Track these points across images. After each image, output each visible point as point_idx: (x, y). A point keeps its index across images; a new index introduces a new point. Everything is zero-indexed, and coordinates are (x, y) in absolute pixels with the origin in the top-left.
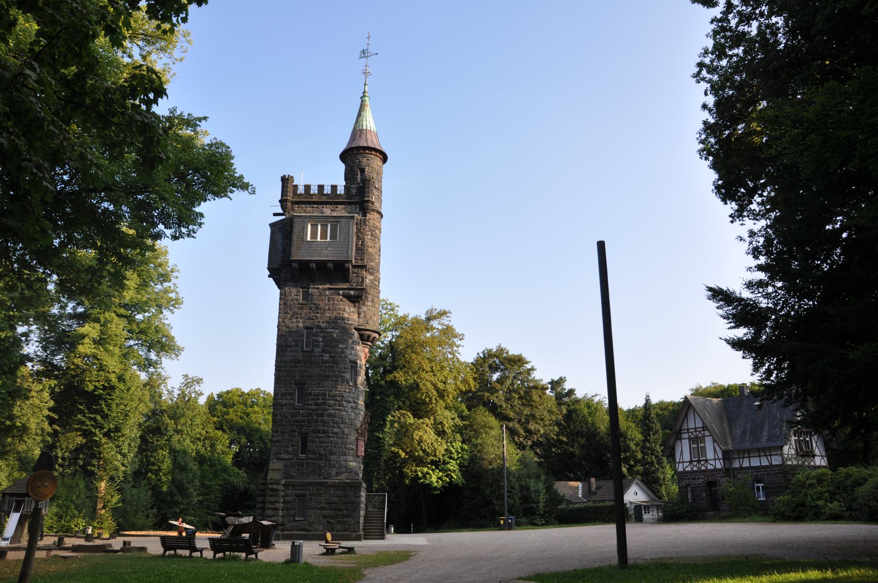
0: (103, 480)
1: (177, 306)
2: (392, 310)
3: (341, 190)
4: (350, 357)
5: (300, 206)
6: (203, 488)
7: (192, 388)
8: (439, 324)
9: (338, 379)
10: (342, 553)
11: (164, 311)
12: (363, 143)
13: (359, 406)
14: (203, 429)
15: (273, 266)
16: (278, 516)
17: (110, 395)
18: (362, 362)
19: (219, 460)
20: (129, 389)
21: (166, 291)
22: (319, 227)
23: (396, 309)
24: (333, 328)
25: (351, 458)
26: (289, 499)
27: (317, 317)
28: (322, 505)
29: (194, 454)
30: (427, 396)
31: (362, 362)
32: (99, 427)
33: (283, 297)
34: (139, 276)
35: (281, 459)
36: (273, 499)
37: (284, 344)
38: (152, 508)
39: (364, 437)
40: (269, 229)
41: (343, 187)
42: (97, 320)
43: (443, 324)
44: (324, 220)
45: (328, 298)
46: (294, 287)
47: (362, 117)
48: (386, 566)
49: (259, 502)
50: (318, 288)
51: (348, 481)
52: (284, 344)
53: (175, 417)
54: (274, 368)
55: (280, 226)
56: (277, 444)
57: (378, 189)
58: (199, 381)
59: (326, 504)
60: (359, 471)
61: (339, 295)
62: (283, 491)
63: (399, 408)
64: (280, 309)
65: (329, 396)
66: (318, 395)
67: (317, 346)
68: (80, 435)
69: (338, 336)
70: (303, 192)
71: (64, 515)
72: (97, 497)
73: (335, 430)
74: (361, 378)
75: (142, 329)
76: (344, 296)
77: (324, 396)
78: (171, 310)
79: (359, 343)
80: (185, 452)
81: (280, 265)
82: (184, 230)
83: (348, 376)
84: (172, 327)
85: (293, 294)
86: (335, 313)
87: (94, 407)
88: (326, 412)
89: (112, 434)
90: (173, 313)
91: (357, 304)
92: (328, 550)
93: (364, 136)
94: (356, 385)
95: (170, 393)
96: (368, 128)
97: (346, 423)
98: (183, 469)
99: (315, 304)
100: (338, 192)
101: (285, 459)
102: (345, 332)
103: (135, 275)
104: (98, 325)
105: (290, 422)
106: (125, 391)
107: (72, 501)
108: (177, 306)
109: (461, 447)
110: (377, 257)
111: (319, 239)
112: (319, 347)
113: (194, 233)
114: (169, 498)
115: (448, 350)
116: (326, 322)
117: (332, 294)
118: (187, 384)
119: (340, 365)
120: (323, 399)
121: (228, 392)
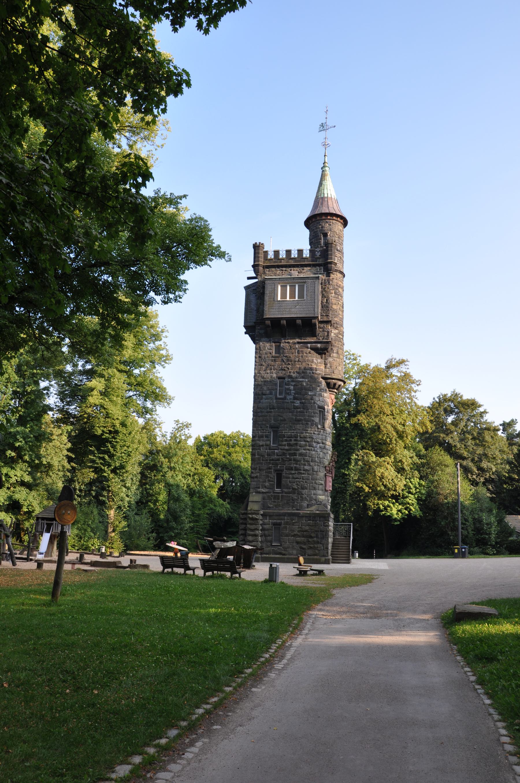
0: (112, 508)
1: (167, 362)
2: (355, 359)
3: (306, 254)
4: (318, 403)
5: (271, 269)
6: (193, 516)
7: (182, 432)
8: (398, 371)
9: (308, 422)
10: (313, 575)
11: (156, 366)
12: (325, 210)
13: (327, 447)
14: (192, 466)
15: (249, 324)
16: (257, 541)
17: (115, 439)
18: (329, 407)
19: (206, 493)
20: (130, 433)
21: (158, 349)
22: (288, 287)
23: (358, 358)
24: (303, 378)
25: (320, 492)
26: (266, 527)
27: (288, 368)
28: (296, 533)
29: (185, 488)
30: (387, 437)
31: (329, 407)
32: (107, 465)
33: (258, 351)
34: (135, 336)
35: (259, 493)
36: (253, 527)
37: (260, 392)
38: (152, 532)
39: (332, 473)
40: (243, 293)
41: (308, 251)
42: (102, 376)
43: (401, 372)
44: (292, 281)
45: (298, 351)
46: (267, 342)
47: (323, 186)
48: (352, 587)
49: (242, 529)
50: (289, 343)
51: (318, 512)
52: (260, 392)
53: (168, 456)
54: (252, 413)
55: (254, 288)
56: (255, 479)
57: (339, 251)
58: (188, 426)
59: (298, 531)
60: (327, 503)
61: (308, 348)
62: (261, 520)
63: (363, 448)
64: (255, 362)
65: (301, 438)
66: (290, 437)
67: (289, 394)
68: (92, 471)
69: (308, 385)
70: (273, 257)
71: (83, 536)
72: (108, 522)
73: (306, 467)
74: (329, 422)
75: (138, 382)
76: (311, 349)
77: (296, 437)
78: (162, 365)
79: (326, 390)
80: (178, 486)
81: (255, 323)
82: (171, 296)
83: (317, 420)
84: (164, 380)
85: (266, 348)
86: (304, 364)
87: (102, 449)
88: (298, 452)
89: (118, 471)
90: (164, 368)
91: (323, 356)
92: (300, 571)
93: (325, 203)
94: (324, 427)
95: (163, 436)
96: (329, 196)
97: (315, 461)
98: (177, 500)
99: (286, 357)
100: (304, 256)
101: (263, 493)
102: (313, 380)
103: (132, 336)
104: (103, 379)
105: (267, 460)
106: (127, 435)
107: (88, 525)
108: (167, 362)
109: (419, 483)
110: (341, 313)
111: (288, 299)
112: (291, 395)
113: (180, 298)
114: (165, 525)
115: (407, 395)
116: (296, 372)
117: (301, 347)
118: (178, 428)
119: (310, 410)
120: (295, 440)
121: (212, 435)
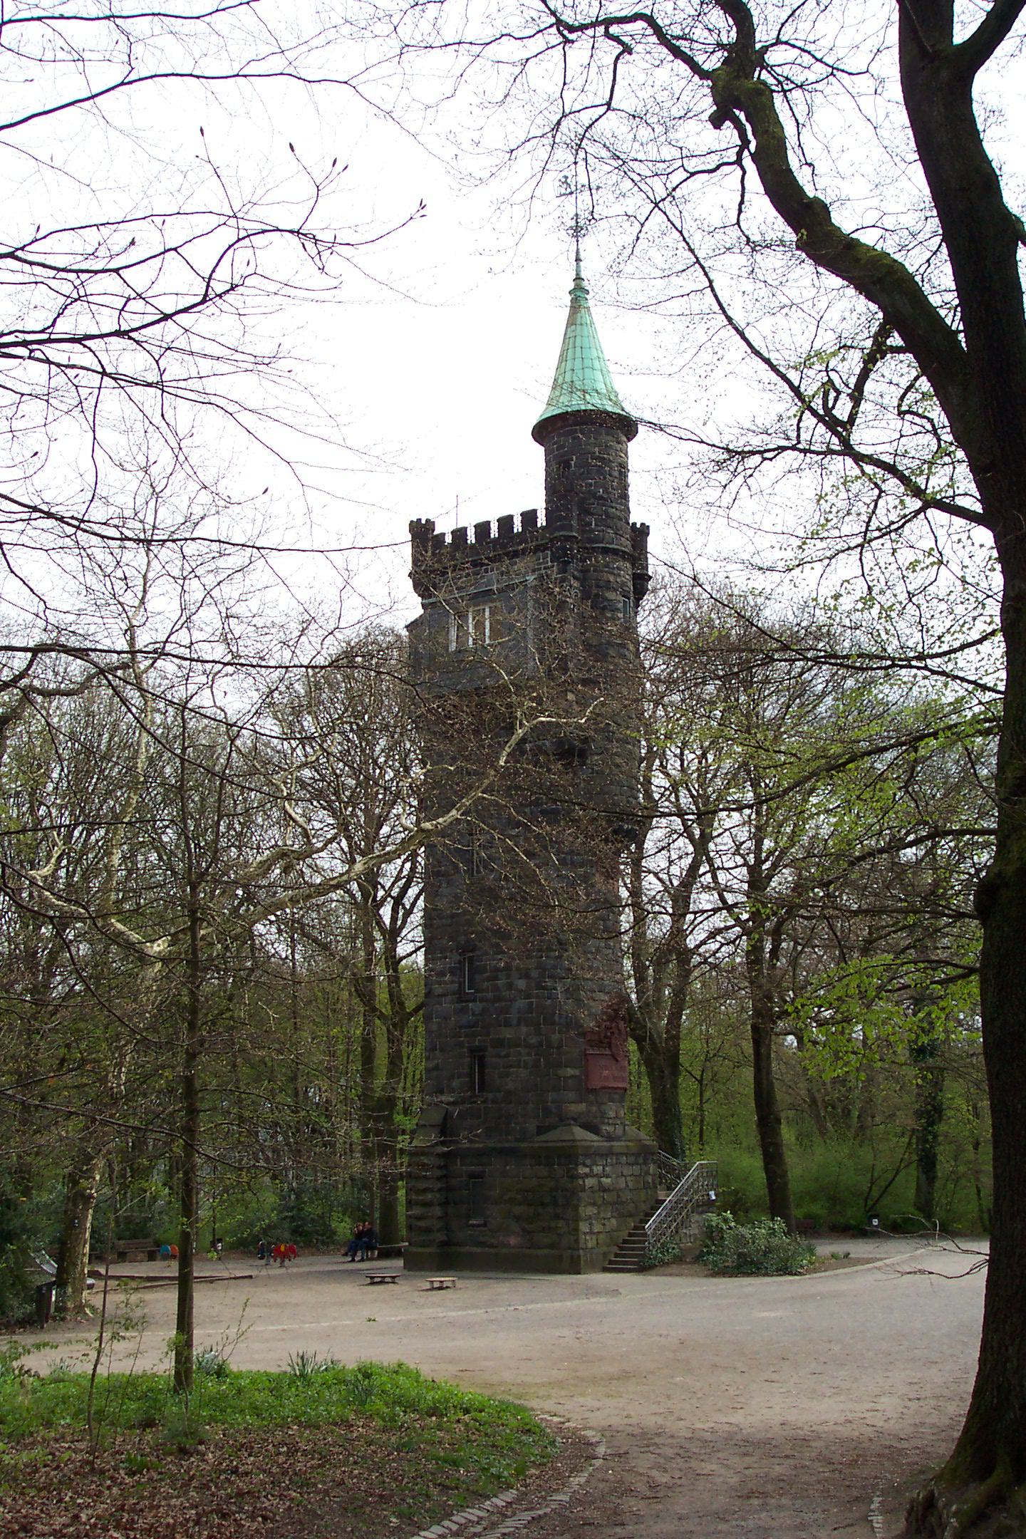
97: (554, 1023)
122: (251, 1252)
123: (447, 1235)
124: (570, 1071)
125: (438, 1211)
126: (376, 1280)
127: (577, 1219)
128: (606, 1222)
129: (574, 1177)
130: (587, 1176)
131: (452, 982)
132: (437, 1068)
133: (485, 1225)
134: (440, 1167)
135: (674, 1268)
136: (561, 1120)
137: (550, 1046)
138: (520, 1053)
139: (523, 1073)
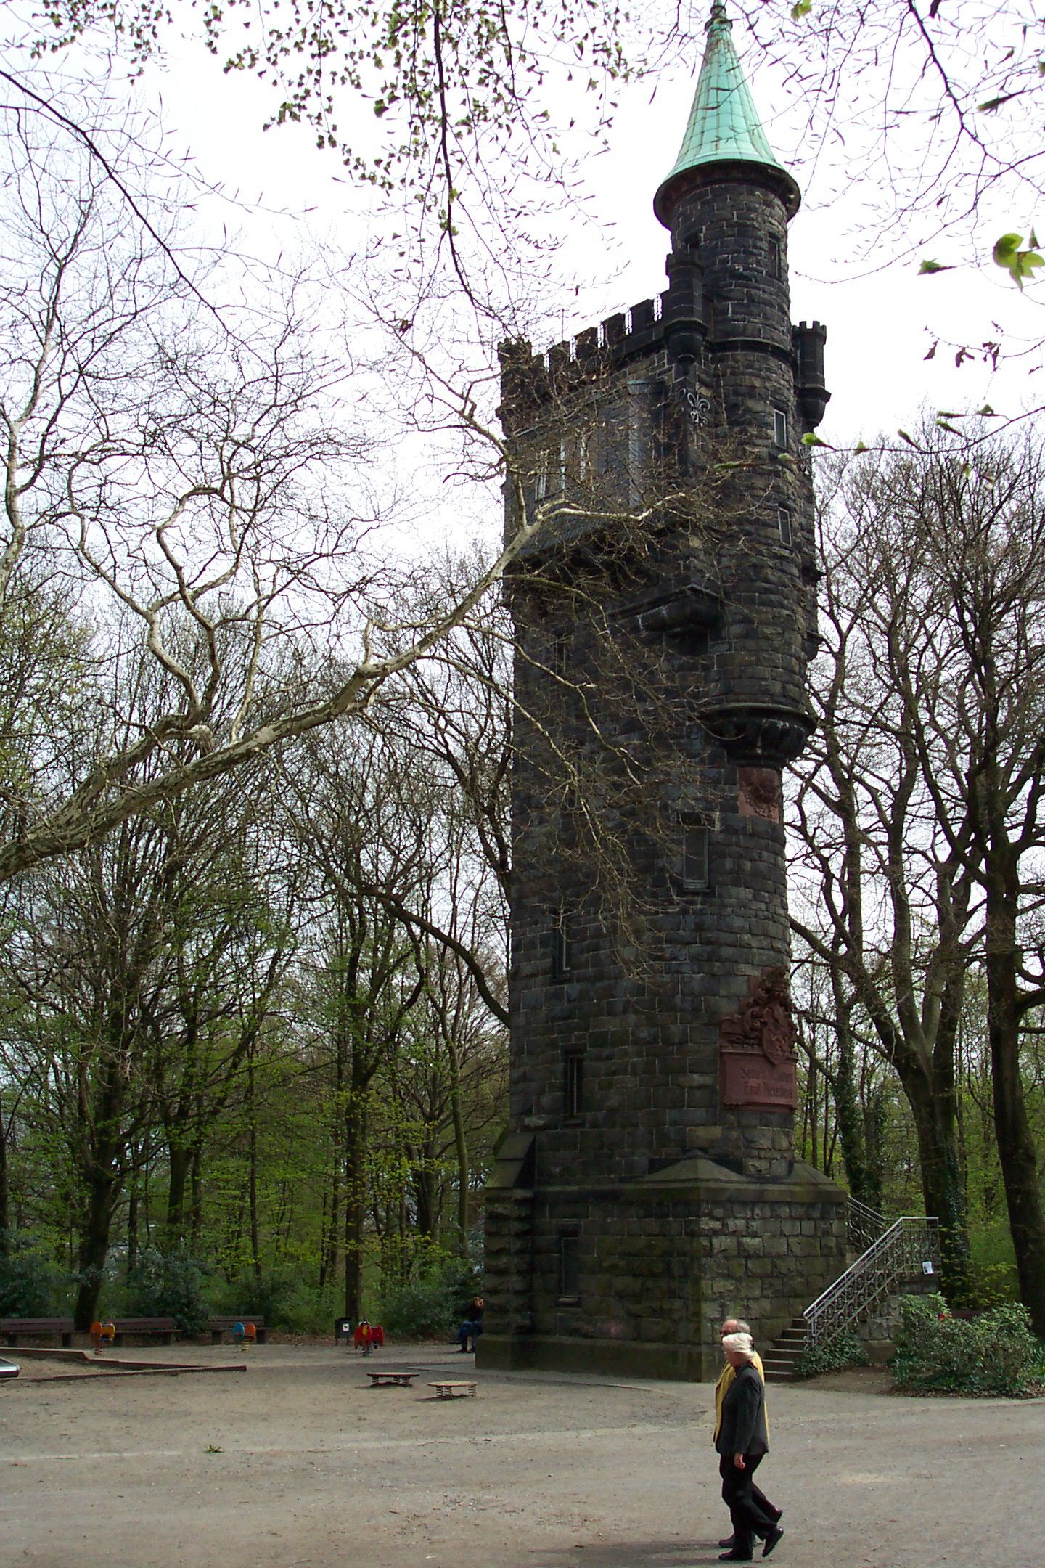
122: (397, 1337)
123: (531, 1318)
124: (698, 1079)
125: (515, 1282)
126: (381, 1381)
127: (699, 1298)
128: (752, 1304)
129: (693, 1235)
130: (715, 1233)
131: (544, 956)
132: (524, 1078)
133: (578, 1304)
134: (519, 1219)
135: (847, 1378)
136: (685, 1151)
137: (667, 1041)
138: (626, 1053)
139: (630, 1081)
